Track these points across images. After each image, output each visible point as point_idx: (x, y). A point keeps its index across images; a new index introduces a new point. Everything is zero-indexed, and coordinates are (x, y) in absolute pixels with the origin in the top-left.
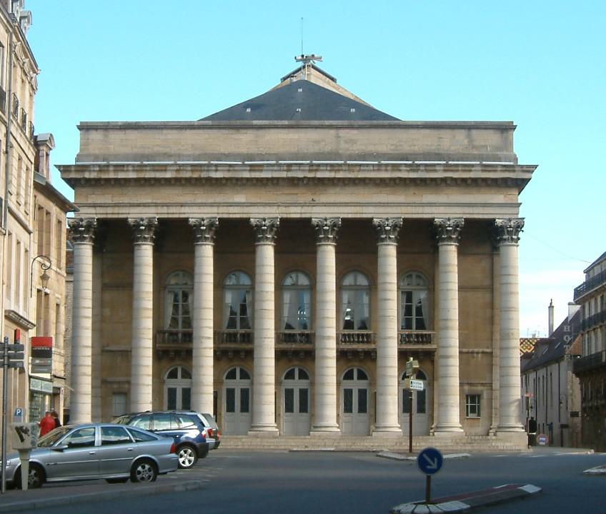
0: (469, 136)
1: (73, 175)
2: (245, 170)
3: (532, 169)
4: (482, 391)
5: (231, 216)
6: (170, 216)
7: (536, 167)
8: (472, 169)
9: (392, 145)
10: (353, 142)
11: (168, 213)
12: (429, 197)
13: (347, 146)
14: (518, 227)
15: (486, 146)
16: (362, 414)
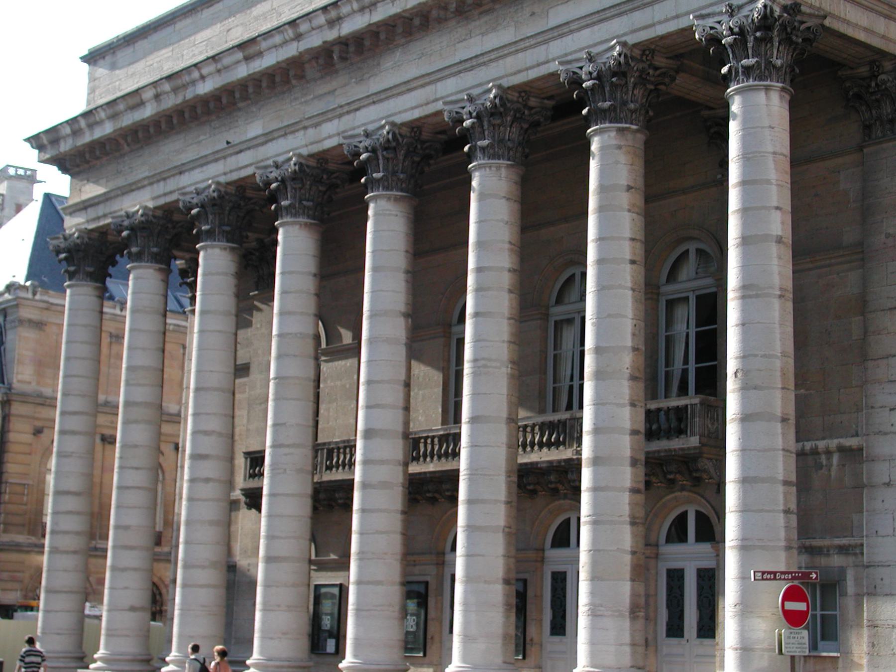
2: (238, 62)
4: (842, 571)
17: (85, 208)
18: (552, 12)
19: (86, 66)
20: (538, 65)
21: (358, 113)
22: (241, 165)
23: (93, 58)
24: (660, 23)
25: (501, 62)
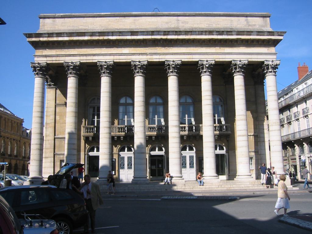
0: (246, 20)
5: (121, 61)
8: (252, 34)
11: (86, 60)
13: (183, 25)
14: (277, 65)
15: (255, 25)
17: (46, 57)
21: (166, 56)
24: (253, 59)
25: (212, 55)
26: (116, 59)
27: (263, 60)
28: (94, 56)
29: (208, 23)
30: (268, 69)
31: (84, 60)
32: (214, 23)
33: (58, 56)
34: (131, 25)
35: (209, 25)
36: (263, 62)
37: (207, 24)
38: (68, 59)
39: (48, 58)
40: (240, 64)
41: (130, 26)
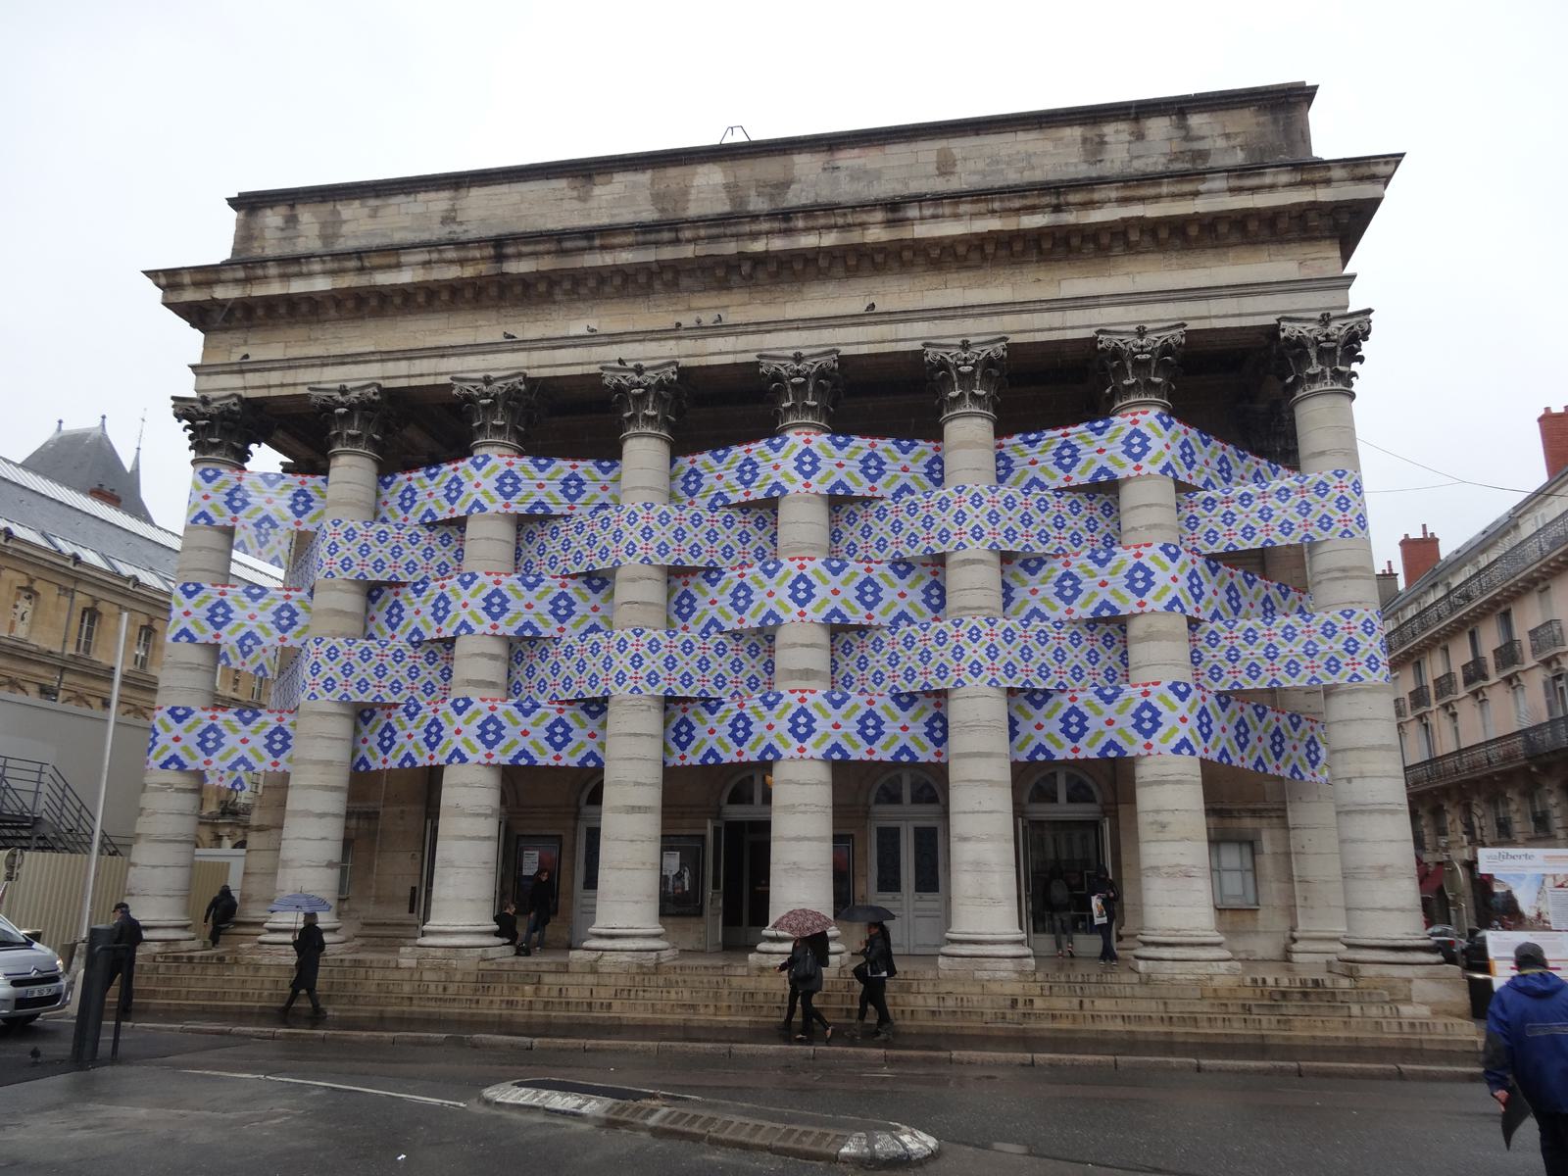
0: (1183, 126)
1: (189, 296)
3: (1381, 170)
6: (415, 382)
7: (1396, 159)
8: (1202, 187)
9: (975, 173)
10: (877, 175)
11: (409, 376)
12: (1076, 283)
16: (927, 896)
18: (1064, 284)
19: (232, 215)
20: (1051, 329)
22: (1244, 311)
23: (248, 204)
24: (1216, 317)
25: (995, 318)
26: (540, 367)
27: (1271, 320)
28: (443, 356)
29: (981, 165)
30: (1303, 359)
31: (400, 374)
32: (1008, 164)
33: (290, 368)
34: (615, 211)
35: (983, 173)
36: (1273, 331)
37: (971, 173)
38: (331, 377)
39: (249, 376)
40: (1142, 347)
41: (613, 216)
